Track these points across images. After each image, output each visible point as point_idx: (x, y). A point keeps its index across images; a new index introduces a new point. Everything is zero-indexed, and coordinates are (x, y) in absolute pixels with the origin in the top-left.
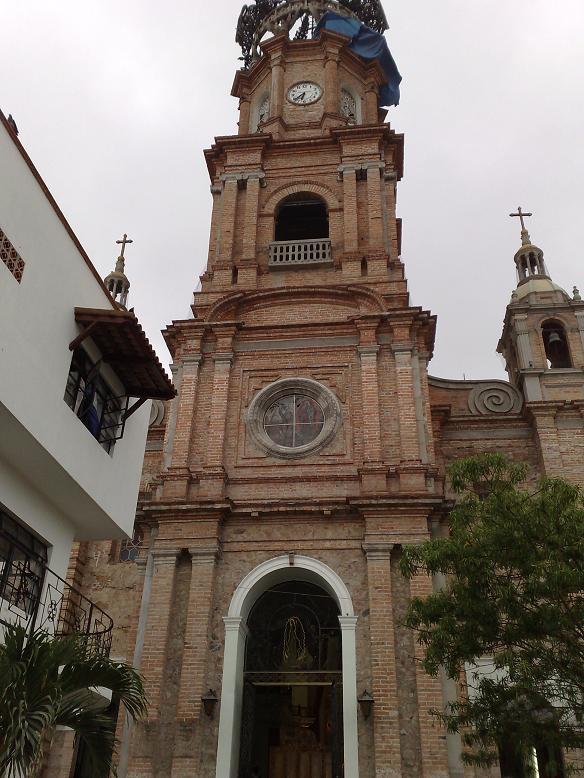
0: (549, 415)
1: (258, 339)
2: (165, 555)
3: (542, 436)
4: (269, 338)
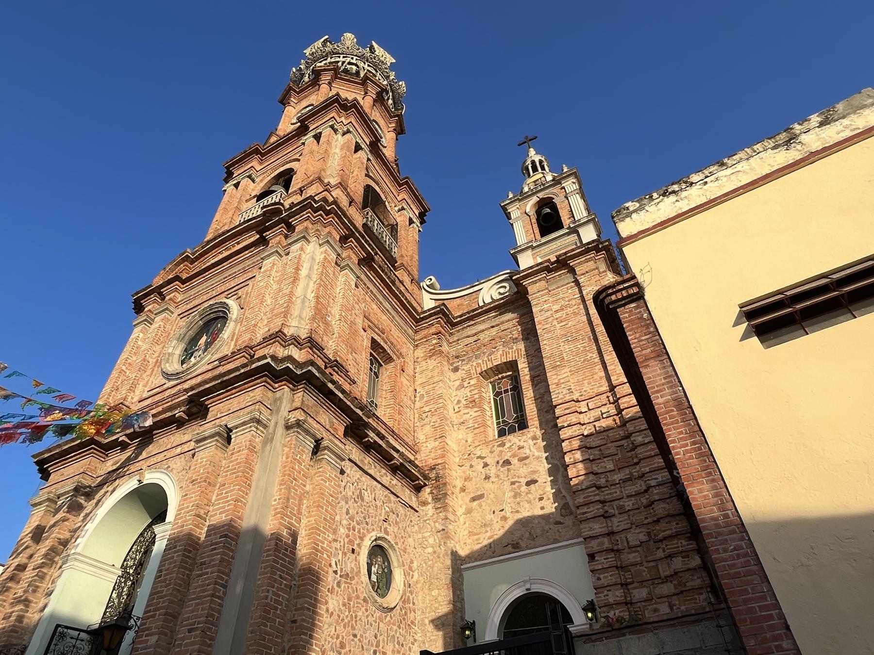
0: (540, 280)
1: (198, 285)
2: (40, 503)
3: (533, 303)
4: (206, 280)
